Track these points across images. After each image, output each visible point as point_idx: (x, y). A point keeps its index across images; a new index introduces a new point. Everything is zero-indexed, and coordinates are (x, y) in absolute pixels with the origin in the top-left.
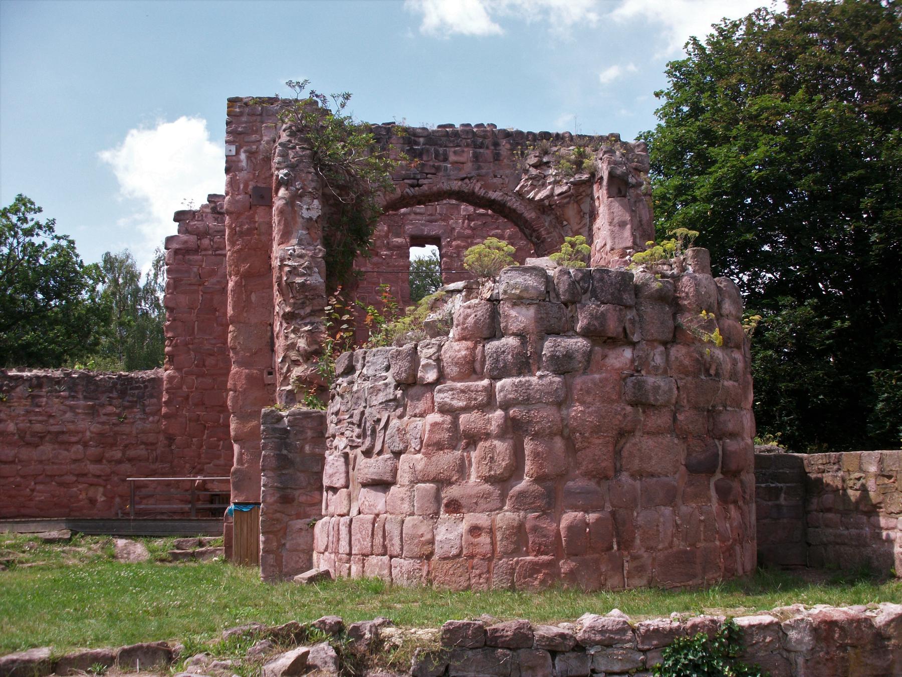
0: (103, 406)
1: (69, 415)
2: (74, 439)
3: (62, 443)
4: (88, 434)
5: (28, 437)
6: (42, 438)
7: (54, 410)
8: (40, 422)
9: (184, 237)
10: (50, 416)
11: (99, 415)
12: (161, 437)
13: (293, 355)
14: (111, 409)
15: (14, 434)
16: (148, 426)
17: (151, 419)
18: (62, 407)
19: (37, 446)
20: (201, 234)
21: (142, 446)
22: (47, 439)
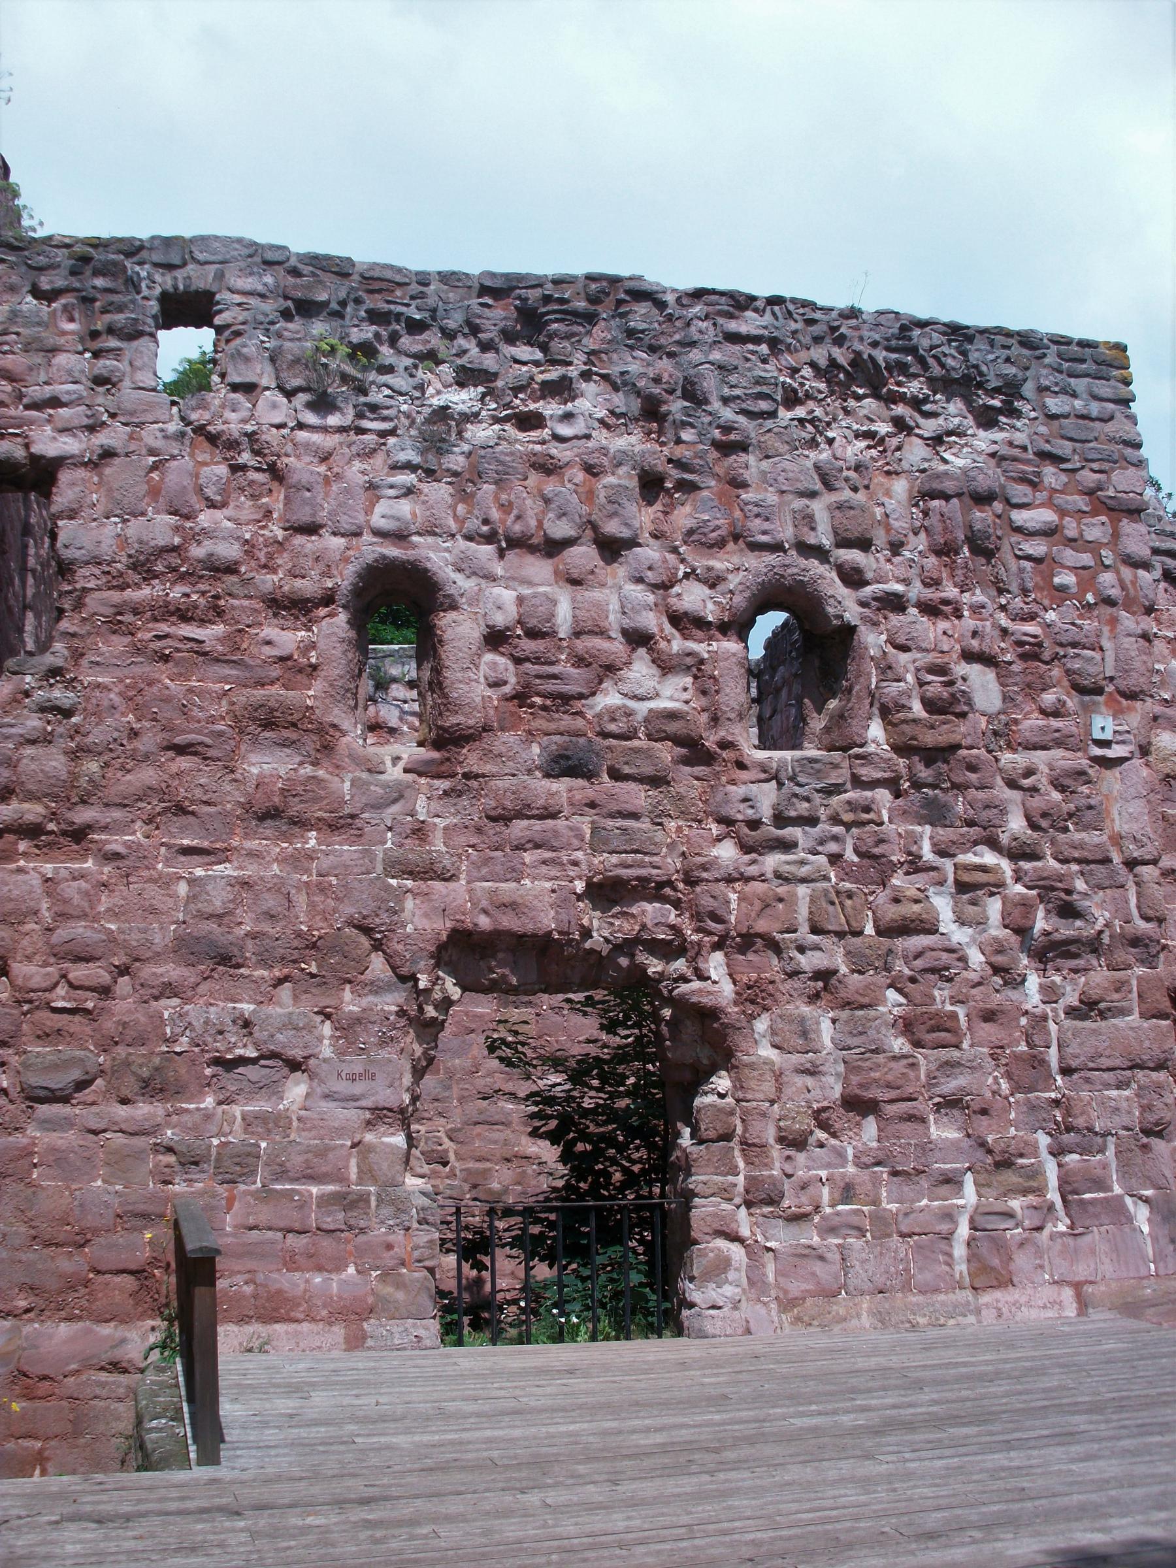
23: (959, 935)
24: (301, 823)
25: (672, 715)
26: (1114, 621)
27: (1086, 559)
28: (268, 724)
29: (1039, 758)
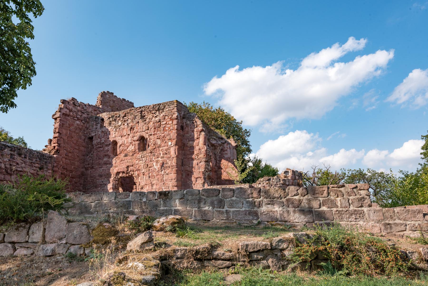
1: (23, 165)
5: (9, 171)
10: (18, 164)
13: (207, 170)
14: (37, 165)
15: (3, 169)
16: (48, 174)
18: (22, 161)
20: (71, 111)
23: (156, 167)
24: (107, 164)
27: (169, 126)
28: (106, 156)
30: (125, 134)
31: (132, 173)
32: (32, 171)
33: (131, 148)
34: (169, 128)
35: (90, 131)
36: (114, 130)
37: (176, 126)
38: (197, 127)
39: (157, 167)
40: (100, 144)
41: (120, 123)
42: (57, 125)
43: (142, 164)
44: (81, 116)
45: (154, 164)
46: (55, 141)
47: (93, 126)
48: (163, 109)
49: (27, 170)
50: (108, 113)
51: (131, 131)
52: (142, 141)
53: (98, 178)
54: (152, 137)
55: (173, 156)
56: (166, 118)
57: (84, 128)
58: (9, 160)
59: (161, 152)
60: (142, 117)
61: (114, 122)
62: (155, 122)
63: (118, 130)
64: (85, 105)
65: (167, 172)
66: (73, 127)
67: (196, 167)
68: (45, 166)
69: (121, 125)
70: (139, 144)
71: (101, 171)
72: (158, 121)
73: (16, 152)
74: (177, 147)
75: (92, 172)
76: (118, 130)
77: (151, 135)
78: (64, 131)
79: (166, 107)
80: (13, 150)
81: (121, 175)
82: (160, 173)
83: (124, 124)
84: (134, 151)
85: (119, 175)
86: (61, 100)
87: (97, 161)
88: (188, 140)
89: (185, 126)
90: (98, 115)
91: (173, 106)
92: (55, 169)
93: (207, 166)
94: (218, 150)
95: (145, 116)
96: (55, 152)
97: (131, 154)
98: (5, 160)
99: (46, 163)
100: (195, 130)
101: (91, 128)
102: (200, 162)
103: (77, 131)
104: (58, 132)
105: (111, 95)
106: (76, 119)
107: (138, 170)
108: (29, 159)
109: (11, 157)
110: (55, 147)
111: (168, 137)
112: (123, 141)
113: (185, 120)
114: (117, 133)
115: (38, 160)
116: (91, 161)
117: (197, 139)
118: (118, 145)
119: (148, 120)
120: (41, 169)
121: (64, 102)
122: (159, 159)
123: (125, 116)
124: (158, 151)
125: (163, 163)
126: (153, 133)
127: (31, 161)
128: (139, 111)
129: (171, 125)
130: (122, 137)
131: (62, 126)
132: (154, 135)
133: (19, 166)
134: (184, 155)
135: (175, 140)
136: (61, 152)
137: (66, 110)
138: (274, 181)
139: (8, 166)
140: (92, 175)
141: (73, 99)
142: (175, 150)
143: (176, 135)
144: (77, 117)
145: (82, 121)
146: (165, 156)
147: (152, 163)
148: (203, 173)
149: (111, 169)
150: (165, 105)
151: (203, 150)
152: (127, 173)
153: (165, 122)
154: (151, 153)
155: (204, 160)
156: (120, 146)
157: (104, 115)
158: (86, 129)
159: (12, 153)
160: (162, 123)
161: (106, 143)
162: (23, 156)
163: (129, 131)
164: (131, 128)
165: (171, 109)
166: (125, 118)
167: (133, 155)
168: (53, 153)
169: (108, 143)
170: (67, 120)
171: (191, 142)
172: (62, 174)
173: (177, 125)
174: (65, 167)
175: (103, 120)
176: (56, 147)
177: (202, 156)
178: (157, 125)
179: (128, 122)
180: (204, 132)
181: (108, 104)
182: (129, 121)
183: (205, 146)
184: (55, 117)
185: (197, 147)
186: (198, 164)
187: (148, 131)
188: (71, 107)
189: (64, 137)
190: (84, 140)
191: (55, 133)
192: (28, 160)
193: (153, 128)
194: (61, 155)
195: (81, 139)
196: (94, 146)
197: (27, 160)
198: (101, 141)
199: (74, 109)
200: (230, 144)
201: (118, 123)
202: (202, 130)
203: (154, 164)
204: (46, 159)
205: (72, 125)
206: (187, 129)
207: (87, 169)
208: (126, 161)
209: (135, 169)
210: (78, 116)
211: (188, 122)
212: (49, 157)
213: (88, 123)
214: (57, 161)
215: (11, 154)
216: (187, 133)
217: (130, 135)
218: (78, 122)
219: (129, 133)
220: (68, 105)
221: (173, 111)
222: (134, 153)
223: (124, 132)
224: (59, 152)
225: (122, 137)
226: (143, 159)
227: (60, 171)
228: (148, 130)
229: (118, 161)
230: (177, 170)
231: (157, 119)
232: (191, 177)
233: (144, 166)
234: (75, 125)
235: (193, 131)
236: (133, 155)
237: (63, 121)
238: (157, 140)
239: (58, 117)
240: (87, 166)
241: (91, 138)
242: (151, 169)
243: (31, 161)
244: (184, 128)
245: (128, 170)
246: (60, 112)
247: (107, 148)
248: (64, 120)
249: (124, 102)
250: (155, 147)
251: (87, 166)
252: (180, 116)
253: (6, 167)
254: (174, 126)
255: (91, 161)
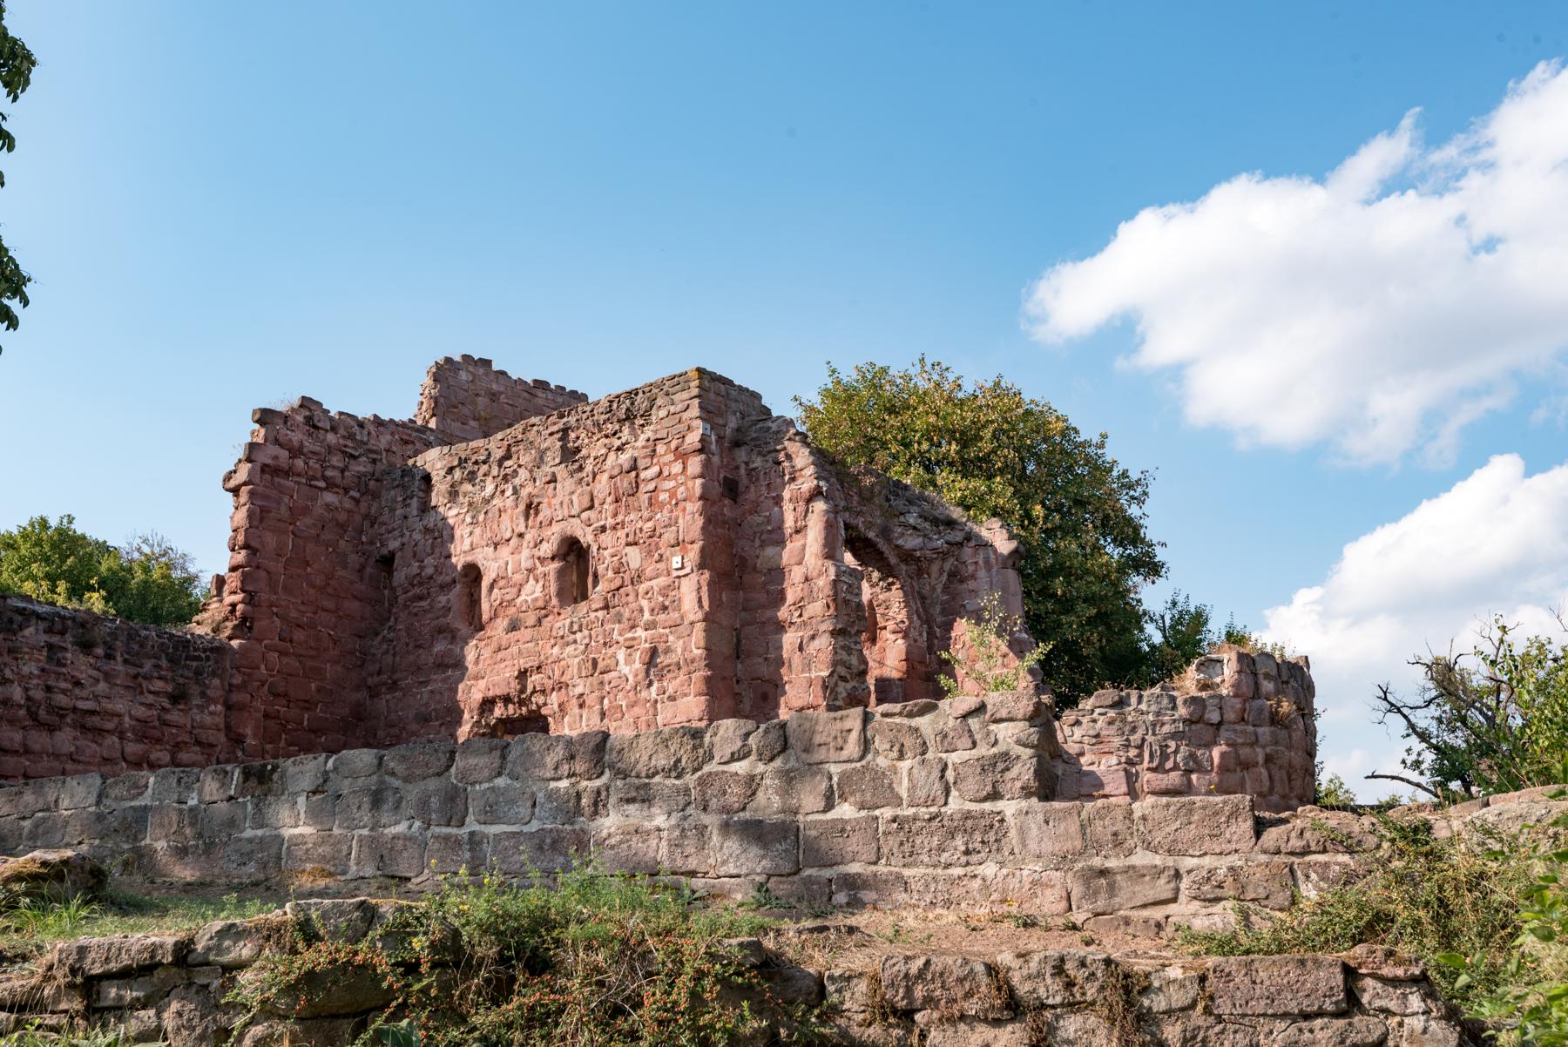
0: (147, 678)
1: (102, 687)
2: (110, 726)
3: (84, 728)
4: (127, 719)
5: (42, 713)
6: (62, 716)
7: (82, 676)
8: (64, 692)
9: (274, 450)
10: (77, 683)
11: (142, 693)
12: (222, 738)
13: (842, 671)
14: (159, 685)
15: (20, 706)
16: (208, 720)
17: (212, 708)
18: (94, 673)
19: (51, 729)
20: (296, 452)
21: (197, 748)
22: (68, 720)
23: (625, 669)
24: (448, 666)
25: (536, 600)
26: (684, 510)
27: (672, 484)
28: (440, 632)
29: (654, 583)
30: (508, 535)
31: (541, 700)
32: (141, 712)
33: (533, 592)
34: (673, 494)
35: (383, 530)
36: (468, 520)
37: (699, 482)
38: (793, 479)
39: (629, 667)
40: (421, 584)
41: (490, 488)
42: (243, 512)
43: (572, 657)
44: (342, 471)
45: (621, 656)
46: (234, 581)
47: (392, 510)
48: (646, 414)
49: (120, 706)
50: (446, 449)
51: (527, 518)
52: (571, 558)
53: (414, 727)
54: (606, 539)
55: (691, 617)
56: (661, 449)
57: (358, 518)
58: (43, 670)
59: (645, 603)
60: (570, 454)
61: (467, 487)
62: (616, 472)
63: (481, 517)
64: (361, 424)
65: (670, 691)
66: (308, 521)
67: (797, 659)
68: (195, 690)
69: (492, 496)
70: (561, 574)
71: (426, 696)
72: (626, 467)
73: (69, 638)
74: (707, 575)
75: (391, 704)
76: (481, 517)
77: (603, 529)
78: (271, 540)
79: (659, 402)
80: (58, 626)
81: (499, 711)
82: (644, 694)
83: (503, 492)
84: (540, 603)
85: (492, 711)
86: (254, 412)
87: (411, 658)
88: (757, 543)
89: (744, 481)
90: (410, 462)
91: (685, 395)
92: (236, 697)
93: (843, 655)
94: (936, 579)
95: (578, 450)
96: (235, 627)
97: (531, 620)
98: (26, 670)
99: (198, 673)
100: (786, 494)
101: (385, 517)
102: (813, 637)
103: (327, 536)
104: (246, 546)
105: (481, 371)
106: (322, 484)
107: (561, 686)
108: (126, 661)
109: (49, 658)
110: (233, 605)
111: (669, 536)
112: (501, 563)
113: (742, 454)
114: (478, 531)
115: (164, 663)
116: (389, 659)
117: (797, 532)
118: (485, 584)
119: (589, 468)
120: (178, 698)
121: (265, 417)
122: (640, 633)
123: (508, 456)
124: (631, 598)
125: (654, 652)
126: (610, 522)
127: (133, 671)
128: (555, 428)
129: (681, 479)
130: (496, 545)
131: (262, 519)
132: (614, 528)
133: (84, 693)
134: (744, 609)
135: (697, 546)
136: (261, 624)
137: (276, 450)
138: (1143, 707)
139: (38, 694)
140: (393, 716)
141: (306, 403)
142: (699, 588)
143: (700, 521)
144: (324, 478)
145: (346, 490)
146: (662, 617)
147: (610, 651)
148: (825, 687)
149: (461, 687)
150: (653, 392)
151: (823, 583)
152: (522, 703)
153: (656, 469)
154: (606, 607)
155: (828, 626)
156: (492, 587)
157: (433, 460)
158: (366, 524)
159: (55, 639)
160: (643, 475)
161: (440, 579)
162: (100, 651)
163: (522, 520)
164: (529, 506)
165: (679, 407)
166: (507, 463)
167: (539, 621)
168: (228, 633)
169: (448, 579)
170: (281, 490)
171: (770, 551)
172: (266, 716)
173: (701, 476)
174: (281, 690)
175: (427, 478)
176: (240, 607)
177: (816, 608)
178: (624, 483)
179: (517, 481)
180: (827, 498)
181: (465, 411)
182: (523, 474)
183: (829, 563)
184: (232, 484)
185: (796, 569)
186: (801, 649)
187: (592, 514)
188: (296, 437)
189: (271, 565)
190: (360, 571)
191: (233, 550)
192: (120, 667)
193: (609, 500)
194: (260, 641)
195: (345, 567)
196: (399, 591)
197: (119, 666)
198: (422, 568)
199: (309, 445)
200: (987, 545)
201: (483, 488)
202: (816, 494)
203: (621, 656)
204: (198, 658)
205: (306, 511)
206: (752, 495)
207: (374, 693)
208: (514, 649)
209: (549, 684)
210: (329, 473)
211: (758, 462)
212: (212, 650)
213: (376, 496)
214: (243, 661)
215: (51, 647)
216: (755, 510)
217: (528, 537)
218: (329, 497)
219: (522, 529)
220: (284, 431)
221: (685, 416)
222: (544, 612)
223: (503, 527)
224: (250, 628)
225: (496, 545)
226: (579, 636)
227: (258, 704)
228: (591, 507)
229: (486, 653)
230: (708, 680)
231: (625, 458)
232: (777, 706)
233: (579, 669)
234: (318, 510)
235: (778, 500)
236: (539, 621)
237: (265, 497)
238: (628, 549)
239: (245, 484)
240: (376, 679)
241: (387, 562)
242: (607, 677)
243: (133, 671)
244: (741, 488)
245: (522, 691)
246: (249, 460)
247: (443, 599)
248: (268, 491)
249: (539, 393)
250: (618, 583)
251: (376, 679)
252: (720, 438)
253: (29, 699)
254: (690, 484)
255: (389, 659)
